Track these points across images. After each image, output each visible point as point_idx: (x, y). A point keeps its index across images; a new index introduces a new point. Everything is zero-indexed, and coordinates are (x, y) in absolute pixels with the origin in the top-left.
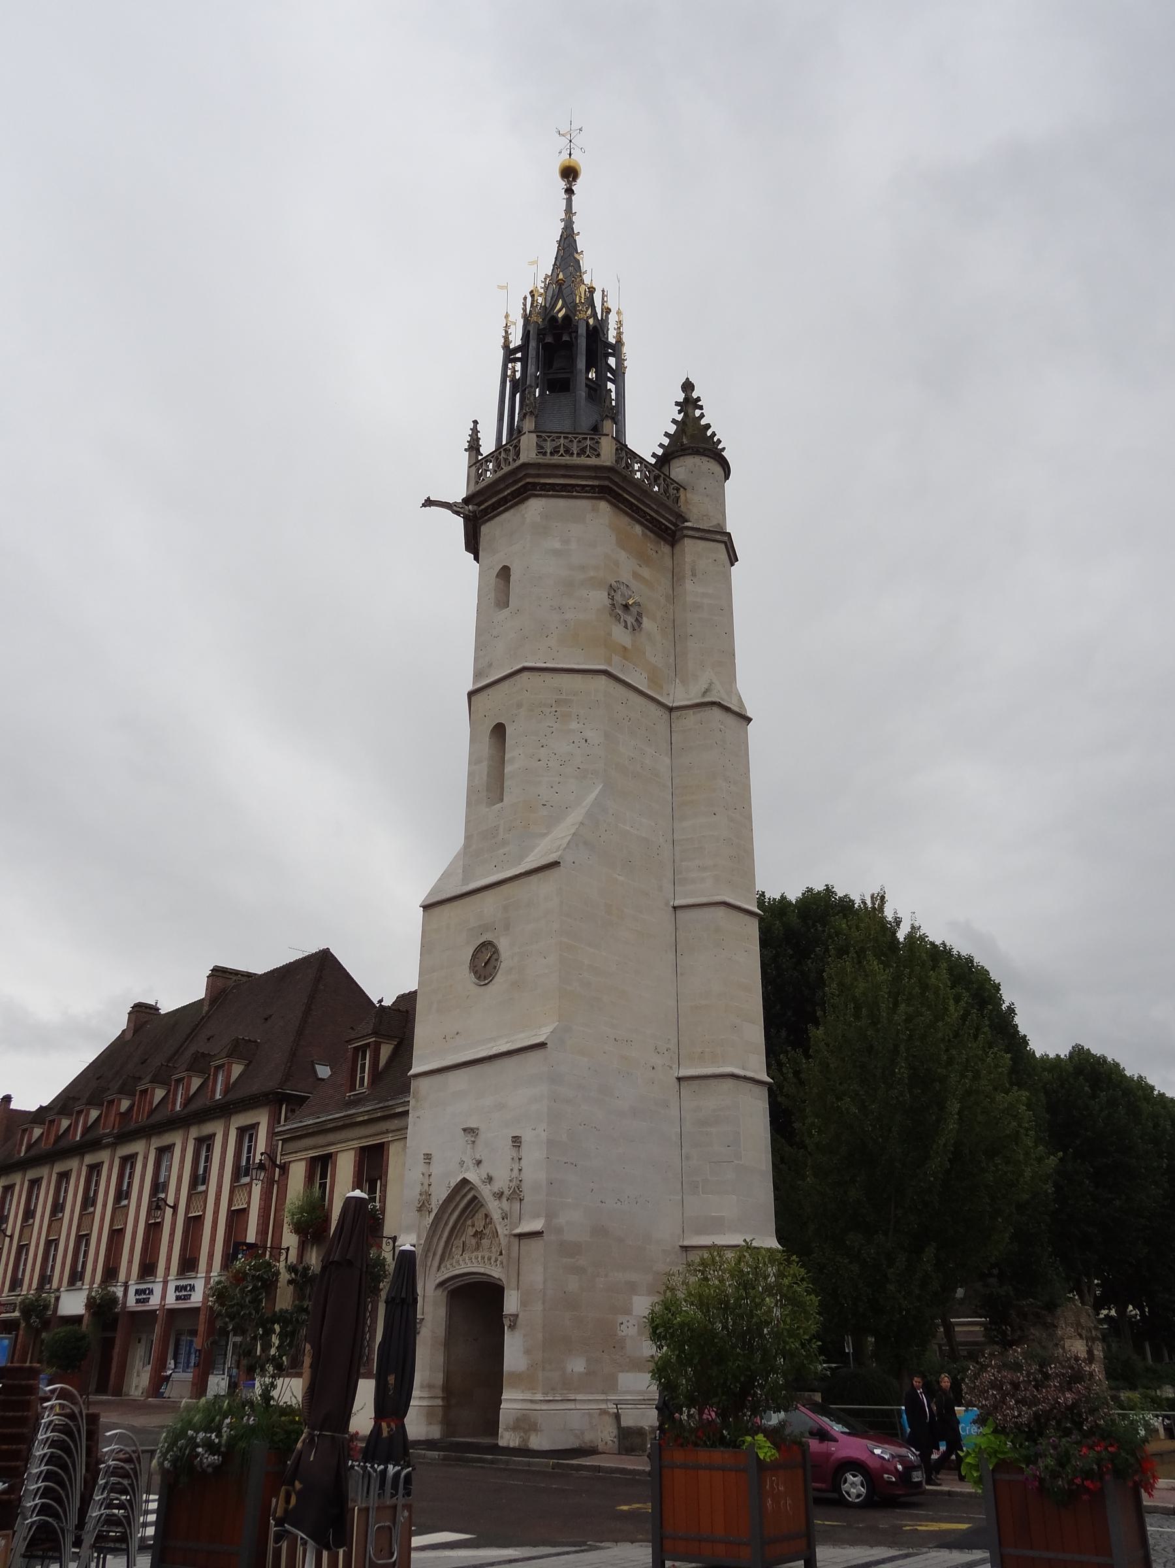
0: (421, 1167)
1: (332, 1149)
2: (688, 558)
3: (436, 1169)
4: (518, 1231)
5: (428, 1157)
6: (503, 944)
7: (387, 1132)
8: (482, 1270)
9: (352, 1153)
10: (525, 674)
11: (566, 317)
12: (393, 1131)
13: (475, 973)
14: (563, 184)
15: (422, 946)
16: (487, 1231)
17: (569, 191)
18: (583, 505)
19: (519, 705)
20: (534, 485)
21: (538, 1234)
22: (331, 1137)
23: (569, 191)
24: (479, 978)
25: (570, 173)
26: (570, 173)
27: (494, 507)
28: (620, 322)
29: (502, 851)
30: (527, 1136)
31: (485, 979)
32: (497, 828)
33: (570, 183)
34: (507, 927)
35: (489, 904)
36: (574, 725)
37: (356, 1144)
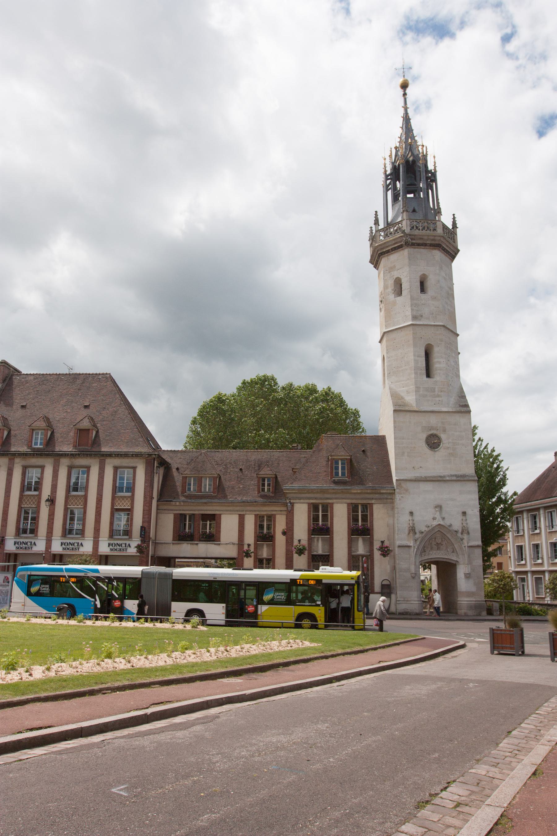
0: (407, 517)
1: (330, 501)
3: (417, 518)
4: (470, 544)
5: (411, 513)
6: (443, 436)
7: (373, 499)
9: (346, 505)
10: (443, 328)
12: (376, 499)
13: (428, 445)
15: (395, 427)
16: (444, 543)
17: (405, 94)
19: (441, 340)
23: (405, 94)
24: (431, 447)
25: (404, 86)
26: (404, 86)
27: (419, 245)
29: (437, 399)
30: (469, 512)
31: (434, 448)
32: (434, 389)
33: (405, 91)
35: (433, 420)
37: (349, 501)
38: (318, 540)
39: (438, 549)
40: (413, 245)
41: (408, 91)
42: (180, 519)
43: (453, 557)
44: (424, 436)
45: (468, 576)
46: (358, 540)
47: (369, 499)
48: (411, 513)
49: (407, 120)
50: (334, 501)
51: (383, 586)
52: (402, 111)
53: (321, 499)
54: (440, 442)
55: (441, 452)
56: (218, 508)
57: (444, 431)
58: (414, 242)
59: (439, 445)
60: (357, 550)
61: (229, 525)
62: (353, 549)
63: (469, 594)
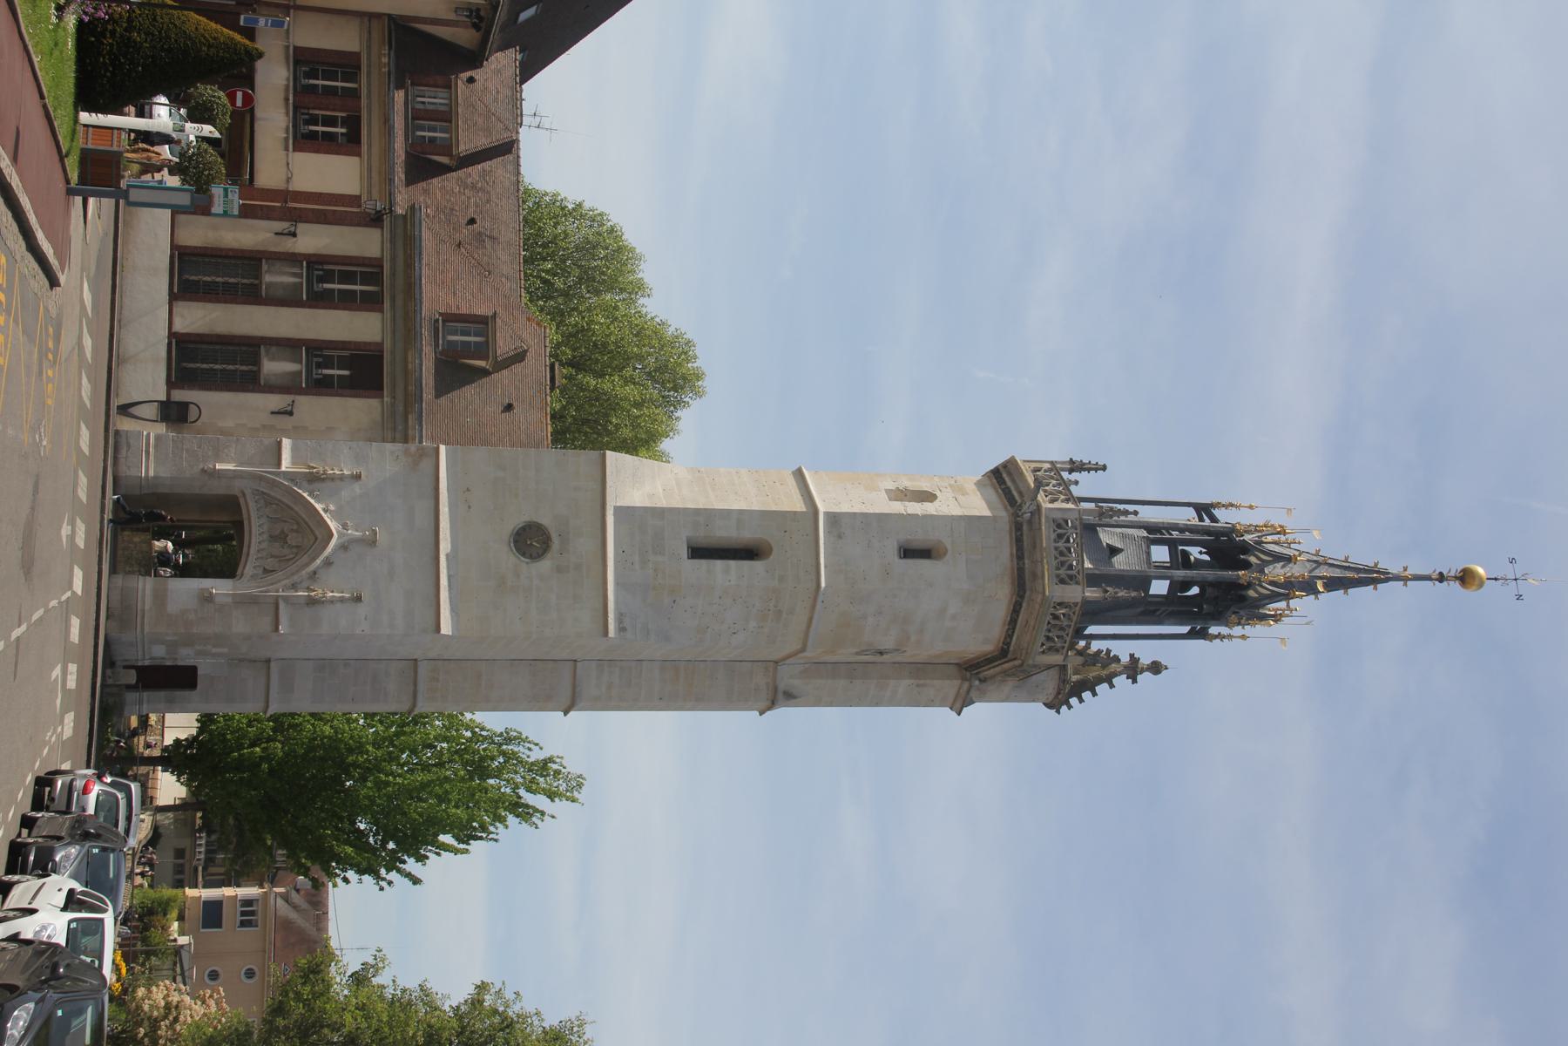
2: (936, 682)
6: (545, 565)
8: (252, 551)
9: (378, 339)
11: (1243, 599)
12: (393, 405)
13: (523, 529)
14: (1454, 568)
17: (1441, 578)
18: (996, 632)
20: (1022, 597)
21: (277, 629)
22: (399, 302)
23: (1441, 578)
25: (1465, 577)
27: (1019, 541)
28: (1230, 637)
30: (362, 610)
31: (516, 542)
34: (559, 570)
36: (753, 624)
37: (387, 346)
38: (295, 275)
39: (273, 538)
40: (1018, 527)
41: (1456, 586)
42: (346, 65)
43: (249, 568)
44: (545, 521)
45: (207, 598)
46: (294, 361)
47: (394, 387)
48: (358, 477)
49: (1371, 577)
50: (388, 314)
51: (184, 407)
52: (1394, 569)
53: (393, 286)
54: (531, 557)
55: (508, 559)
56: (376, 149)
57: (559, 570)
58: (1025, 527)
59: (523, 555)
60: (273, 359)
61: (331, 174)
62: (274, 349)
63: (160, 597)
